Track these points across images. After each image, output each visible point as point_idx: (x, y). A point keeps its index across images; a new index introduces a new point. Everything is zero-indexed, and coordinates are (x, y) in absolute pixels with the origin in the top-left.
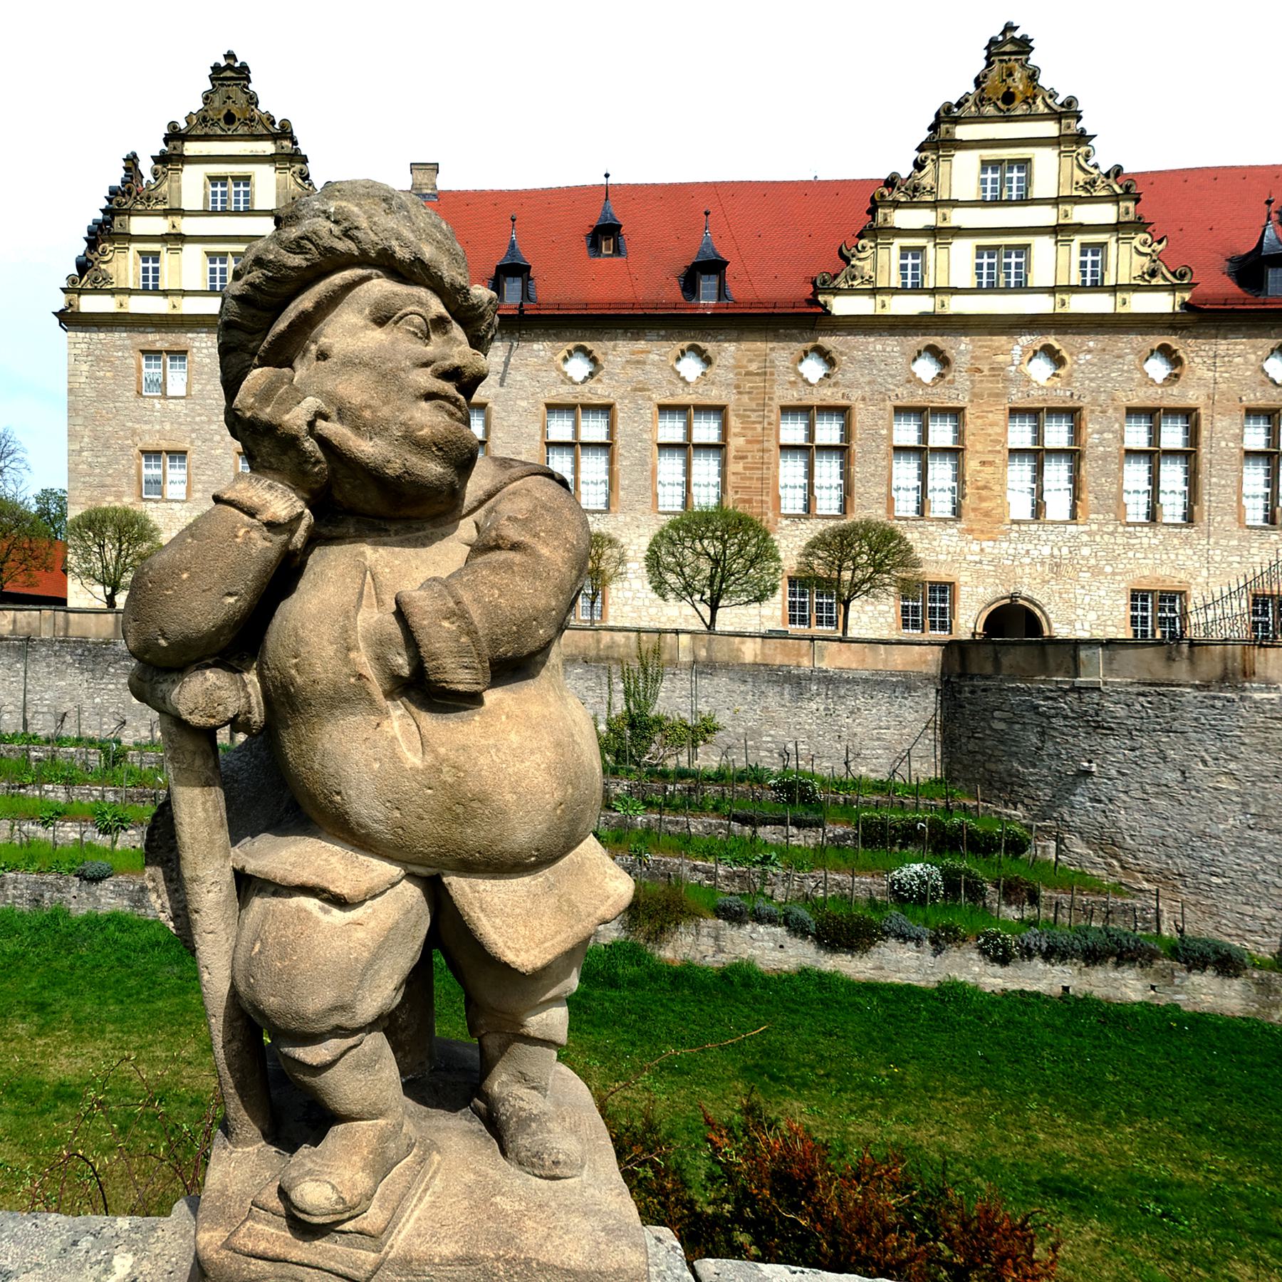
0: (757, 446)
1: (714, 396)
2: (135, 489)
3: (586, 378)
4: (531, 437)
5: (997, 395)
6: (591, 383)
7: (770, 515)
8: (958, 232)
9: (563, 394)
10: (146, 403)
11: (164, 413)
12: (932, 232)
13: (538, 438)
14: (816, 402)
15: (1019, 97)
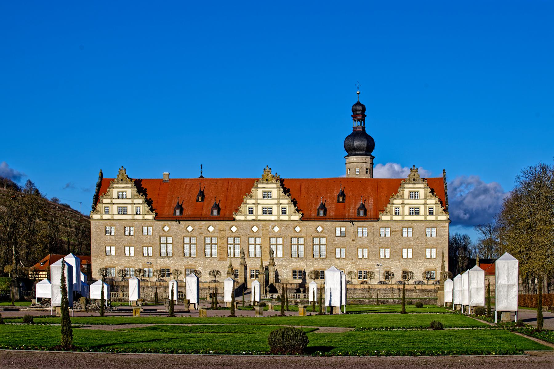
0: (223, 244)
1: (214, 235)
2: (105, 253)
3: (191, 231)
4: (181, 243)
5: (267, 235)
6: (192, 232)
7: (226, 257)
8: (258, 204)
9: (187, 234)
10: (106, 237)
11: (110, 238)
12: (253, 204)
13: (182, 243)
14: (234, 236)
15: (269, 180)
